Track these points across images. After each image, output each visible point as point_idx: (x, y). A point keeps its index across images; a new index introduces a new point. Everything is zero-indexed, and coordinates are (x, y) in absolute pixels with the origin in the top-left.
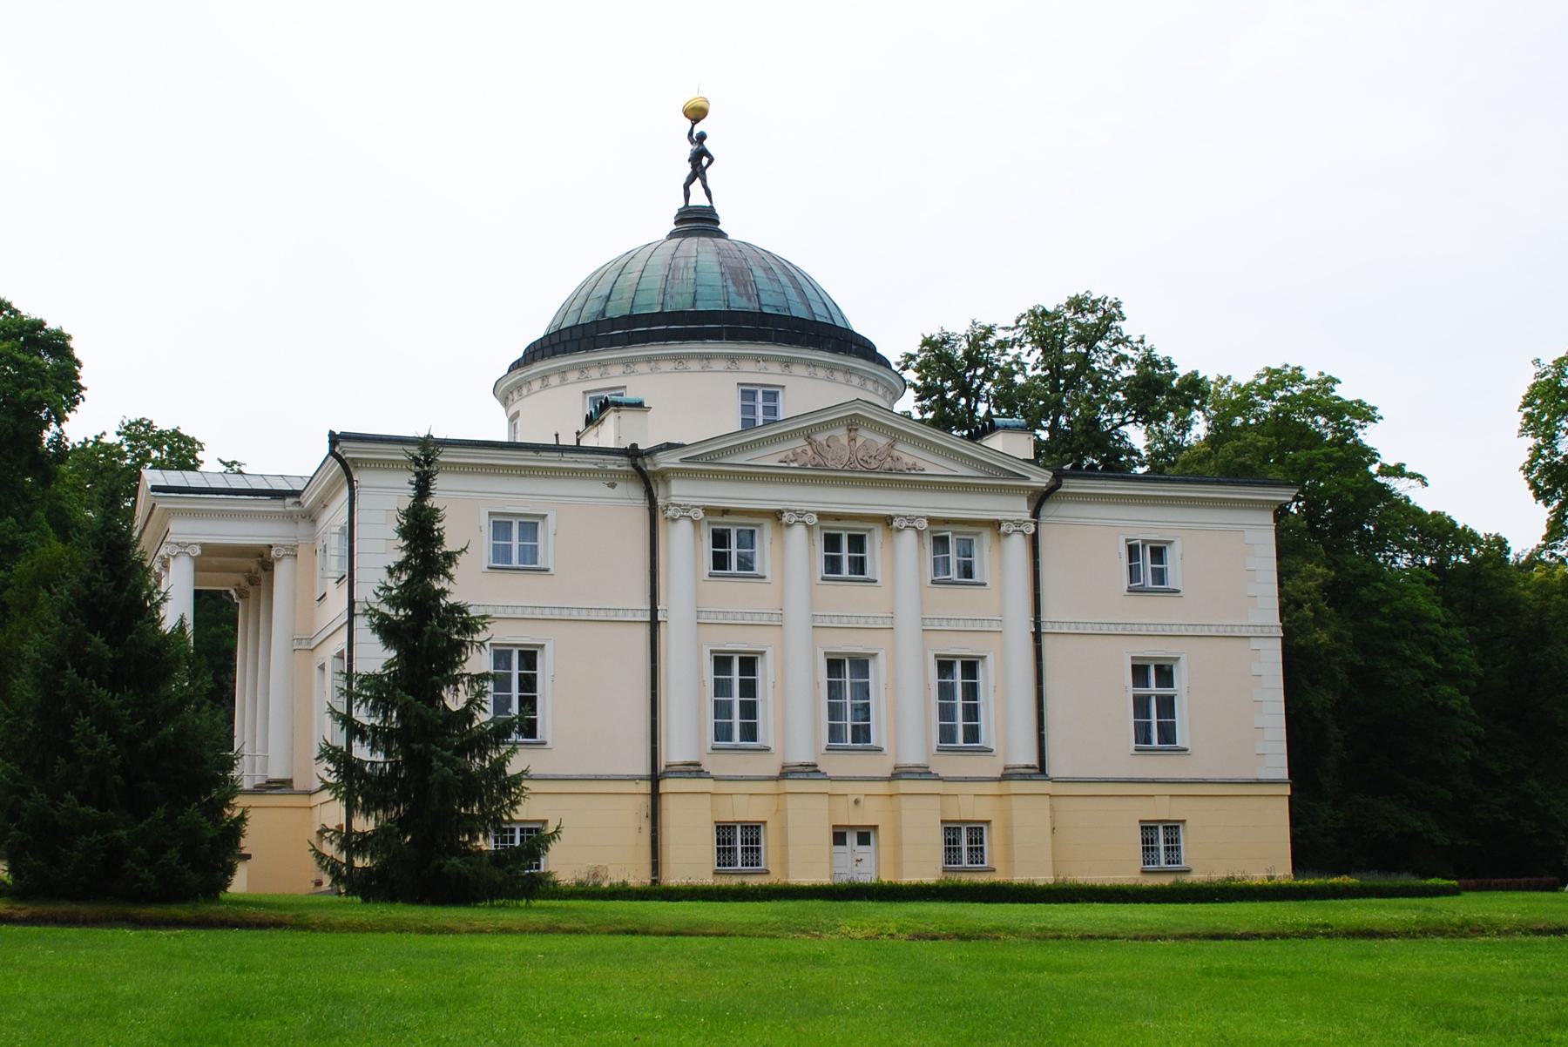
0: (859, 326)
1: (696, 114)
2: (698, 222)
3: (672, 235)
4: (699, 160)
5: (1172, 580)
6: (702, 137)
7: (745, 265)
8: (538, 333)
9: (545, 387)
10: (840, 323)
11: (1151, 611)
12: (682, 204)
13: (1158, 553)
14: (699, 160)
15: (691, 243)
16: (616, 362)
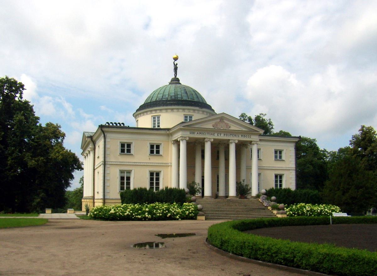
0: (208, 103)
1: (176, 59)
2: (176, 81)
3: (170, 83)
4: (176, 69)
5: (284, 157)
6: (177, 64)
7: (186, 90)
8: (142, 103)
9: (144, 115)
10: (205, 102)
11: (279, 165)
12: (174, 77)
13: (280, 152)
14: (176, 69)
15: (174, 86)
16: (158, 110)
